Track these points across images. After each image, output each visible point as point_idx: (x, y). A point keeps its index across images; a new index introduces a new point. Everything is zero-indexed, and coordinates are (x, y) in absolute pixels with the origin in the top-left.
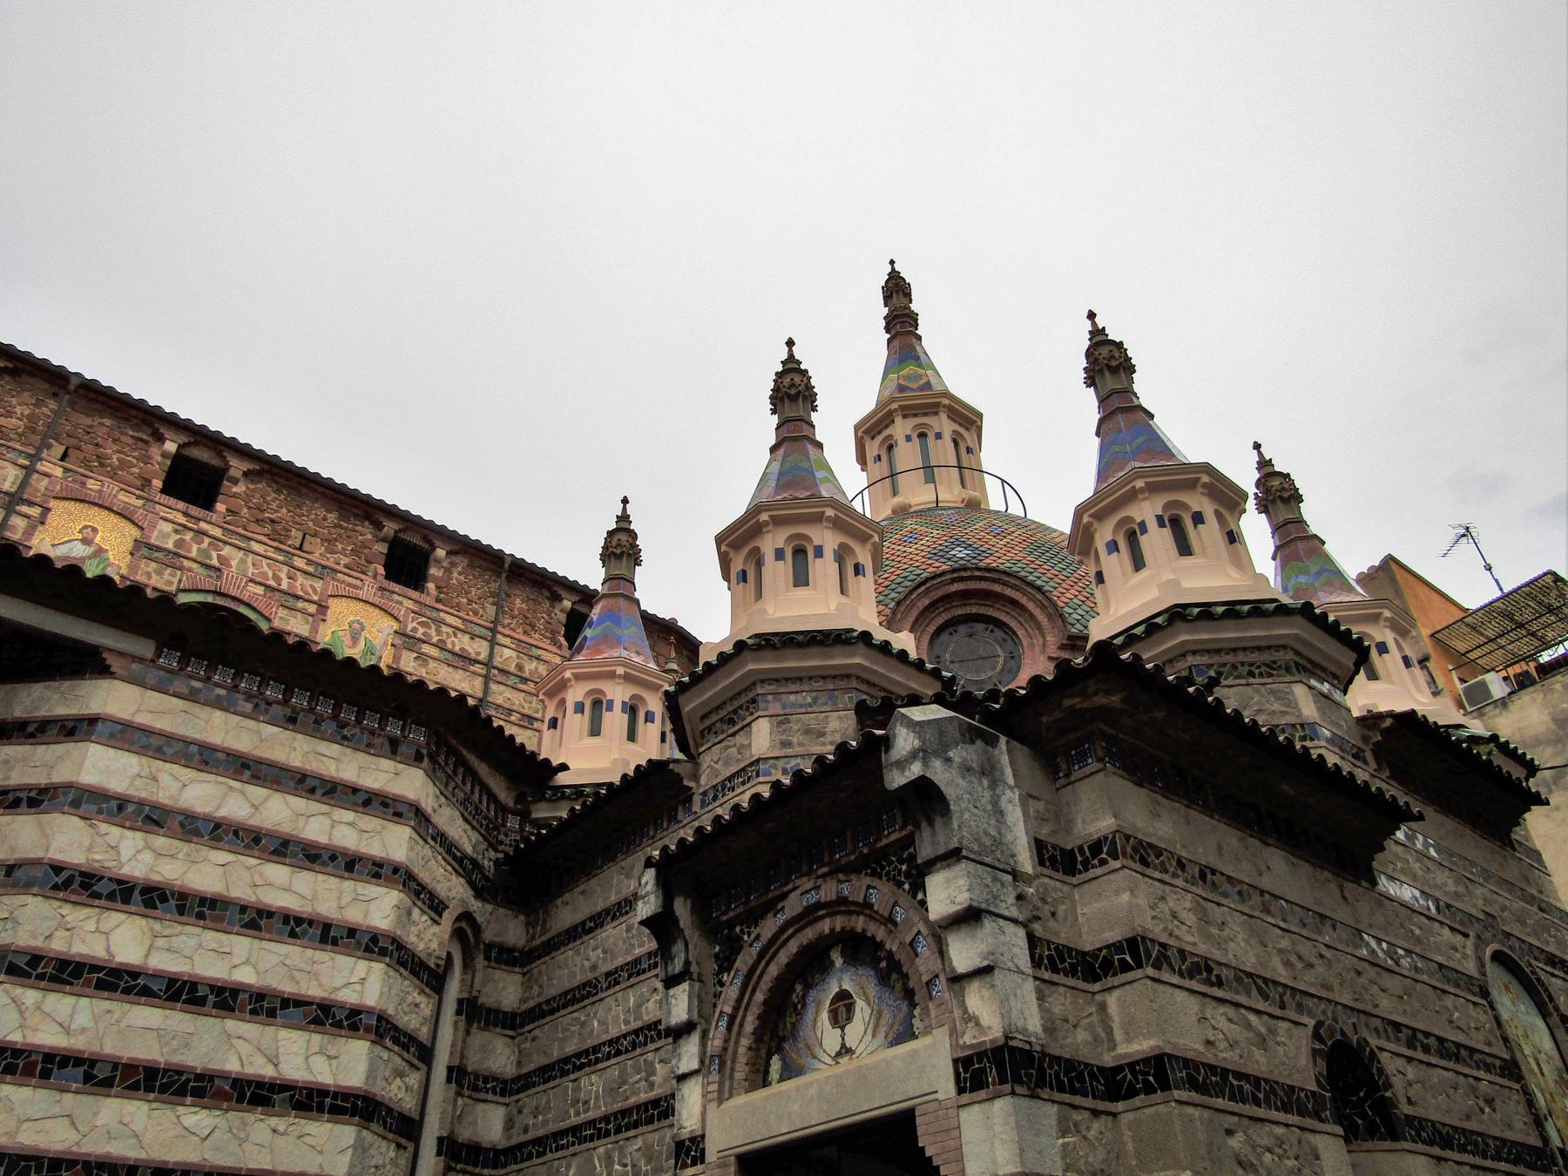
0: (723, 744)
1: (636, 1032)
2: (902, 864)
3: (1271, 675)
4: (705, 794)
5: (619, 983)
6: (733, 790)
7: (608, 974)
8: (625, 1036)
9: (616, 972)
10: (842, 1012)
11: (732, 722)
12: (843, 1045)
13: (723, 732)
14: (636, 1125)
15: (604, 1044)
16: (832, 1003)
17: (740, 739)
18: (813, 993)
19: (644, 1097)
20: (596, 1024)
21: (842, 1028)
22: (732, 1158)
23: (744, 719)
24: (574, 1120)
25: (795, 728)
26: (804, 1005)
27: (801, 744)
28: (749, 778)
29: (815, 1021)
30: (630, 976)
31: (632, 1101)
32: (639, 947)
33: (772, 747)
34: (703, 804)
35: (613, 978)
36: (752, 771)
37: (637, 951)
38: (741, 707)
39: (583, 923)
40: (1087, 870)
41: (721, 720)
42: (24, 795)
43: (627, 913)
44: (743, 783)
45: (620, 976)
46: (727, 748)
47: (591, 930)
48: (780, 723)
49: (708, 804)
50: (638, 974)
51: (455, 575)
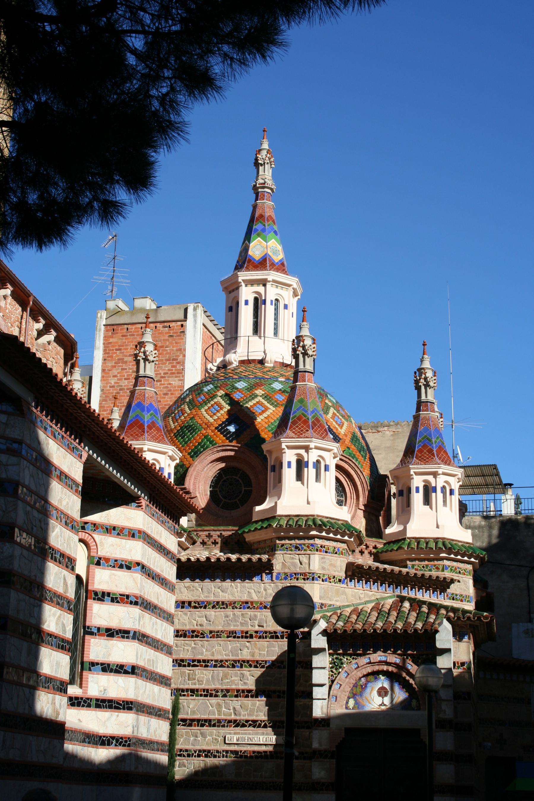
0: (292, 556)
1: (235, 661)
2: (420, 659)
3: (464, 574)
4: (279, 574)
5: (221, 637)
6: (297, 579)
7: (211, 632)
8: (227, 661)
9: (218, 632)
10: (383, 693)
11: (296, 548)
12: (383, 703)
13: (291, 550)
14: (236, 696)
15: (212, 661)
16: (379, 689)
17: (304, 559)
18: (369, 685)
19: (241, 687)
20: (204, 650)
21: (383, 698)
22: (343, 728)
23: (305, 550)
24: (193, 687)
25: (327, 561)
26: (366, 686)
27: (328, 570)
28: (308, 579)
29: (371, 693)
30: (228, 637)
31: (234, 687)
32: (234, 626)
33: (319, 568)
34: (277, 578)
35: (216, 634)
36: (310, 576)
37: (232, 628)
38: (304, 544)
39: (190, 603)
40: (458, 669)
41: (291, 544)
42: (123, 563)
43: (224, 608)
44: (304, 579)
45: (221, 635)
46: (293, 558)
47: (195, 607)
48: (322, 558)
49: (281, 580)
50: (234, 637)
51: (8, 306)
